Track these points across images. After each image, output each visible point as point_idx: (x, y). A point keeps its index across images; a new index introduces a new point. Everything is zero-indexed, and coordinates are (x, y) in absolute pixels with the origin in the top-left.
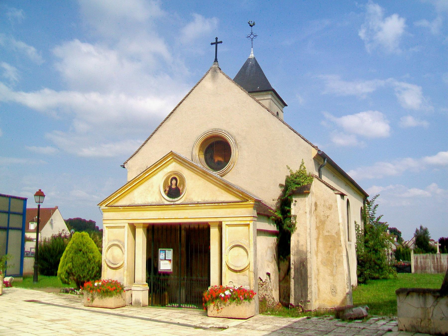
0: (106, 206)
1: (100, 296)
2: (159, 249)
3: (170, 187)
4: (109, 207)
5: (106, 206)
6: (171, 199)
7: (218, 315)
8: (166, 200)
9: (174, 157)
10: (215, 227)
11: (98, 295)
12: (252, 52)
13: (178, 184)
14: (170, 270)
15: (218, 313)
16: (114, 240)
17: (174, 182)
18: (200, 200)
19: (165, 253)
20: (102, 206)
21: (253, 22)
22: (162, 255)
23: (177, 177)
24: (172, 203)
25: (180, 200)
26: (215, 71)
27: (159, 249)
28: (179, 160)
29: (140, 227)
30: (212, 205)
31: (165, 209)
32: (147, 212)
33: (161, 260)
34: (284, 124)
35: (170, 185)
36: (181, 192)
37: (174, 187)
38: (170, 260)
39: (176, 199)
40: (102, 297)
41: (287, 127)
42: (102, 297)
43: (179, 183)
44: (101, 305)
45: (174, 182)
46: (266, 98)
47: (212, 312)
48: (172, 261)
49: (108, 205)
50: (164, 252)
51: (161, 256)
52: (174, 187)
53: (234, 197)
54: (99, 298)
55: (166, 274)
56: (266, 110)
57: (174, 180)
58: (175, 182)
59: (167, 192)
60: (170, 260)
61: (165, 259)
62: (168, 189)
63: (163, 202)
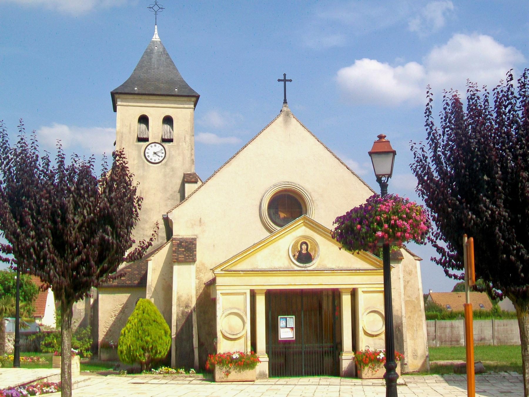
0: (222, 270)
1: (238, 369)
2: (279, 317)
3: (300, 252)
4: (225, 271)
5: (222, 270)
6: (301, 265)
7: (373, 377)
8: (297, 266)
9: (306, 221)
10: (348, 293)
11: (235, 368)
12: (156, 32)
13: (309, 249)
14: (293, 338)
15: (372, 375)
16: (231, 308)
17: (304, 247)
18: (334, 266)
19: (285, 321)
20: (217, 270)
22: (283, 323)
23: (307, 242)
24: (303, 269)
25: (312, 266)
26: (288, 115)
27: (279, 317)
28: (311, 224)
29: (260, 294)
30: (349, 271)
31: (296, 274)
32: (274, 278)
33: (282, 328)
34: (365, 184)
35: (300, 249)
36: (312, 257)
37: (304, 252)
38: (292, 328)
39: (307, 265)
40: (240, 370)
41: (367, 188)
42: (240, 370)
43: (311, 248)
44: (239, 378)
45: (304, 247)
46: (186, 106)
47: (366, 375)
48: (294, 329)
49: (224, 269)
50: (284, 319)
51: (282, 323)
52: (304, 252)
53: (369, 265)
54: (236, 372)
55: (287, 342)
56: (345, 168)
57: (304, 245)
58: (306, 247)
59: (296, 257)
60: (292, 328)
61: (286, 327)
62: (297, 254)
63: (292, 268)
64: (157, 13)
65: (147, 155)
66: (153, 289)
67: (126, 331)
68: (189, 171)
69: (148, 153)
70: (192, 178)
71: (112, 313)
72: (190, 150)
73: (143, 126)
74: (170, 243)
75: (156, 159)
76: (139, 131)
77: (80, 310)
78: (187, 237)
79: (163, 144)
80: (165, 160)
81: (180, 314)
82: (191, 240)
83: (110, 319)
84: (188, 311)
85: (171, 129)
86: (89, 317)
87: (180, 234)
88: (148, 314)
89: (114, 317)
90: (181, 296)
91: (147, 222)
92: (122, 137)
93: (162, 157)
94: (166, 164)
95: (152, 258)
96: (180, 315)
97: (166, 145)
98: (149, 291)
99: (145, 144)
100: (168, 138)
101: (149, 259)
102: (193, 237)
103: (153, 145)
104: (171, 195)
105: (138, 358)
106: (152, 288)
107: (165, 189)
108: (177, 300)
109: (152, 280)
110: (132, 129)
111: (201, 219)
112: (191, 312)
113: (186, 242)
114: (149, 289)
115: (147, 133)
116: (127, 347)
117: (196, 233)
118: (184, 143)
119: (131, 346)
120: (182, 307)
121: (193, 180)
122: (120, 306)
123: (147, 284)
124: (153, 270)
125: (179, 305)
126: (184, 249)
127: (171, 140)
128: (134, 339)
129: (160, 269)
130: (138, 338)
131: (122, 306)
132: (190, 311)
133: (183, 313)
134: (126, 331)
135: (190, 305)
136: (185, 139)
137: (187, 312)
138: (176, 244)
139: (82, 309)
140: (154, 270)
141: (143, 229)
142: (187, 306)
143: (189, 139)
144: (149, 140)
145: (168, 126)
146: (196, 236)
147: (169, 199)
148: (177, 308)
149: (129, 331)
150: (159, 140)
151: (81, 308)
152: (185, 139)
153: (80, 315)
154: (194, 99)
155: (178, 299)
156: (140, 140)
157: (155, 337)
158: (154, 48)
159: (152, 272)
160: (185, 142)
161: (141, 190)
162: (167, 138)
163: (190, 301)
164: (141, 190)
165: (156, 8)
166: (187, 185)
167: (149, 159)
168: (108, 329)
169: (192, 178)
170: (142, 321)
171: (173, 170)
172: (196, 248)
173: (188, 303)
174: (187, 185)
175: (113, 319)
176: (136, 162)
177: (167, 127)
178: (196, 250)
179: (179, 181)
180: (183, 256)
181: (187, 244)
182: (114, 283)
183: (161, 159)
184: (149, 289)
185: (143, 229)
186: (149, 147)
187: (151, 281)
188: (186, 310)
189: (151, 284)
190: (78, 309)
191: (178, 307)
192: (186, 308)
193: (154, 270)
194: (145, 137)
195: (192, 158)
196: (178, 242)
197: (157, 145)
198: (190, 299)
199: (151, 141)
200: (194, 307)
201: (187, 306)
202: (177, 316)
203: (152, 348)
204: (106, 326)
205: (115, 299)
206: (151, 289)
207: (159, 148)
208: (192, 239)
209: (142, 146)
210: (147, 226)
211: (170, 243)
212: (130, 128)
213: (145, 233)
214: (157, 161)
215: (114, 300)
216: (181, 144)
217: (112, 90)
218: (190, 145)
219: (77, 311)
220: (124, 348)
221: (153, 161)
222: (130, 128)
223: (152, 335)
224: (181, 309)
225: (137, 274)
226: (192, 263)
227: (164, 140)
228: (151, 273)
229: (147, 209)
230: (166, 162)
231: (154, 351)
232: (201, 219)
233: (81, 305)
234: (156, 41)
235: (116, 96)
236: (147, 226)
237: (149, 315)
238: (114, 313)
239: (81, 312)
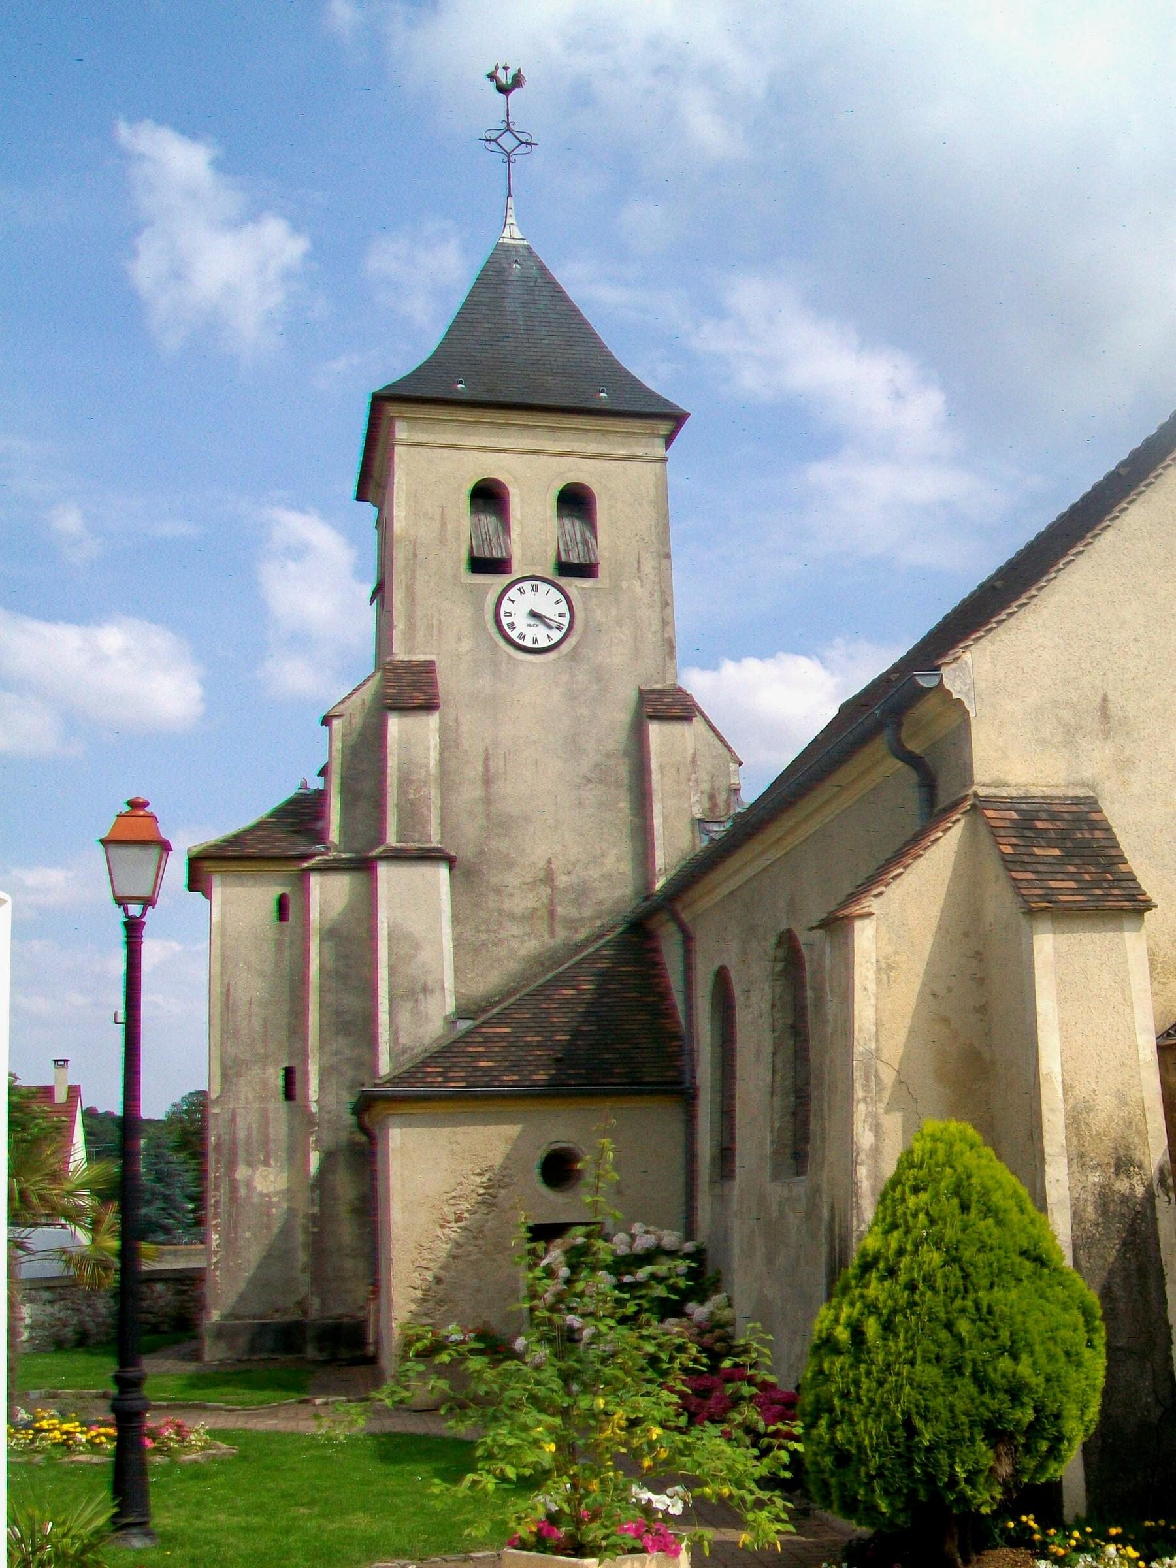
21: (511, 73)
64: (512, 159)
65: (505, 621)
66: (888, 1076)
67: (872, 1327)
68: (657, 683)
69: (508, 614)
70: (671, 705)
71: (446, 1209)
72: (658, 609)
73: (489, 522)
74: (962, 822)
75: (542, 637)
76: (477, 537)
77: (267, 1195)
78: (1049, 792)
79: (563, 581)
80: (572, 641)
81: (1090, 1209)
82: (1074, 808)
83: (439, 1232)
84: (1132, 1187)
85: (588, 534)
86: (300, 1221)
87: (1011, 779)
88: (989, 1211)
89: (453, 1225)
90: (1089, 1109)
91: (511, 865)
92: (415, 556)
93: (559, 628)
94: (574, 656)
95: (872, 904)
96: (1090, 1213)
97: (576, 586)
98: (866, 1087)
99: (498, 581)
100: (582, 560)
101: (856, 909)
102: (1081, 792)
103: (527, 585)
104: (597, 765)
105: (962, 1499)
106: (880, 1065)
107: (573, 746)
108: (1066, 1127)
109: (878, 1024)
110: (449, 527)
111: (1105, 699)
112: (1150, 1197)
113: (1054, 816)
114: (867, 1078)
115: (505, 543)
116: (890, 1428)
117: (1087, 774)
118: (637, 583)
119: (918, 1422)
120: (1094, 1168)
121: (676, 711)
122: (478, 1180)
123: (858, 1048)
124: (879, 969)
125: (1079, 1159)
126: (1057, 852)
127: (586, 570)
128: (930, 1374)
129: (920, 967)
130: (959, 1369)
131: (485, 1179)
132: (1140, 1191)
133: (1104, 1199)
134: (872, 1327)
135: (1138, 1155)
136: (639, 569)
137: (1125, 1199)
138: (1007, 823)
139: (276, 1194)
140: (890, 967)
141: (498, 891)
142: (1123, 1164)
143: (654, 568)
144: (515, 564)
145: (578, 524)
146: (1093, 787)
147: (590, 781)
148: (1070, 1174)
149: (888, 1327)
150: (549, 571)
151: (271, 1189)
152: (639, 569)
153: (269, 1215)
154: (664, 428)
155: (1075, 1122)
156: (481, 565)
157: (1051, 1358)
158: (511, 267)
159: (879, 982)
160: (639, 578)
161: (487, 749)
162: (576, 561)
163: (1138, 1132)
164: (487, 749)
165: (508, 142)
166: (655, 730)
167: (514, 635)
168: (429, 1276)
169: (671, 705)
170: (967, 1254)
171: (599, 674)
172: (1117, 846)
173: (1127, 1148)
174: (655, 730)
175: (453, 1231)
176: (466, 645)
177: (574, 527)
178: (1122, 856)
179: (621, 715)
180: (1072, 885)
181: (1061, 825)
182: (452, 1084)
183: (557, 636)
184: (867, 1078)
185: (498, 891)
186: (513, 593)
187: (873, 1029)
188: (1121, 1185)
189: (877, 1049)
190: (262, 1195)
191: (1075, 1167)
192: (1117, 1172)
193: (885, 968)
194: (497, 554)
195: (666, 635)
196: (1014, 815)
197: (543, 587)
198: (1134, 1124)
199: (517, 571)
200: (1161, 1170)
201: (1123, 1164)
202: (1077, 1217)
203: (1034, 1430)
204: (424, 1263)
205: (456, 1147)
206: (877, 1076)
207: (547, 601)
208: (1077, 801)
209: (486, 589)
210: (512, 880)
211: (962, 822)
212: (443, 525)
213: (506, 906)
214: (544, 643)
215: (453, 1153)
216: (624, 585)
217: (377, 388)
218: (657, 588)
219: (256, 1200)
220: (869, 1431)
221: (528, 643)
222: (443, 525)
223: (1038, 1348)
224: (1095, 1178)
225: (540, 1045)
226: (1127, 924)
227: (566, 569)
228: (872, 987)
229: (511, 817)
230: (575, 648)
231: (1044, 1446)
232: (1105, 699)
233: (272, 1177)
234: (515, 247)
235: (393, 409)
236: (512, 880)
237: (999, 1223)
238: (453, 1209)
239: (270, 1205)
